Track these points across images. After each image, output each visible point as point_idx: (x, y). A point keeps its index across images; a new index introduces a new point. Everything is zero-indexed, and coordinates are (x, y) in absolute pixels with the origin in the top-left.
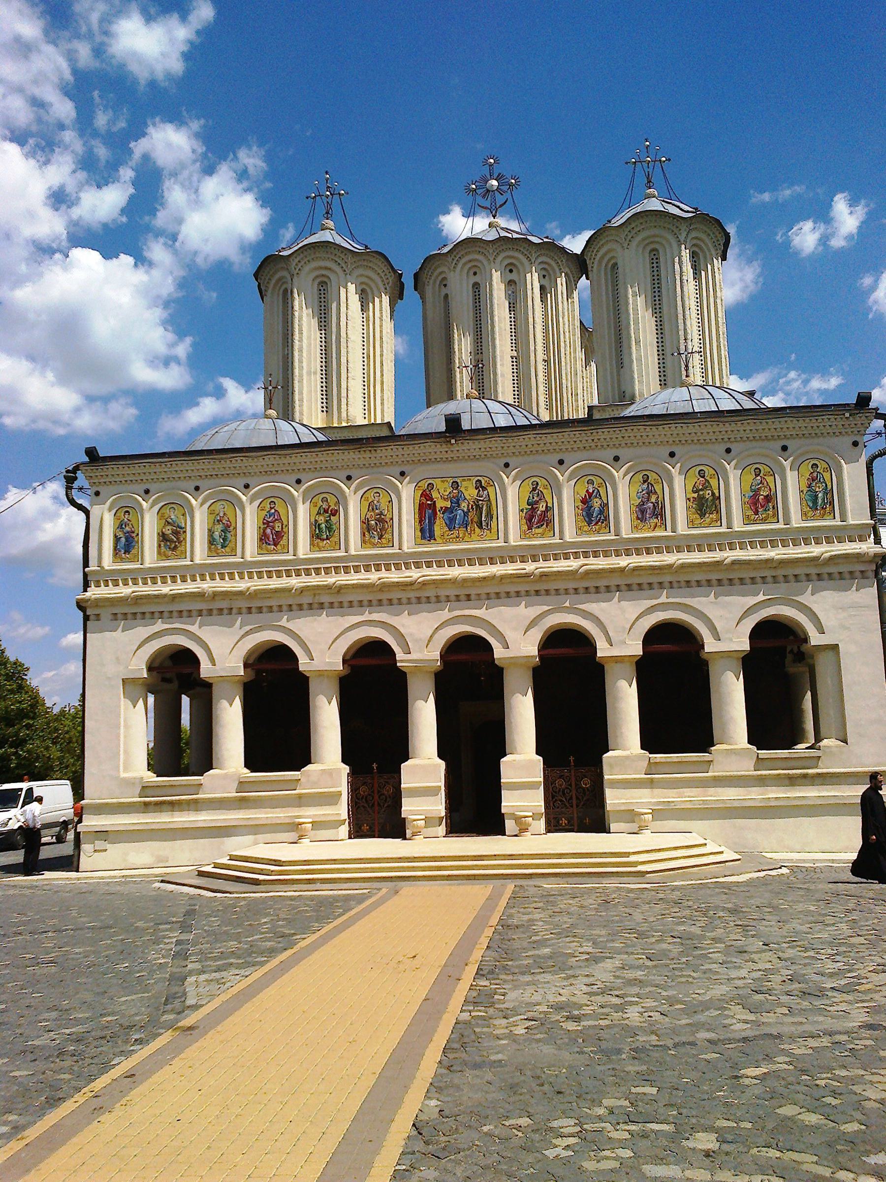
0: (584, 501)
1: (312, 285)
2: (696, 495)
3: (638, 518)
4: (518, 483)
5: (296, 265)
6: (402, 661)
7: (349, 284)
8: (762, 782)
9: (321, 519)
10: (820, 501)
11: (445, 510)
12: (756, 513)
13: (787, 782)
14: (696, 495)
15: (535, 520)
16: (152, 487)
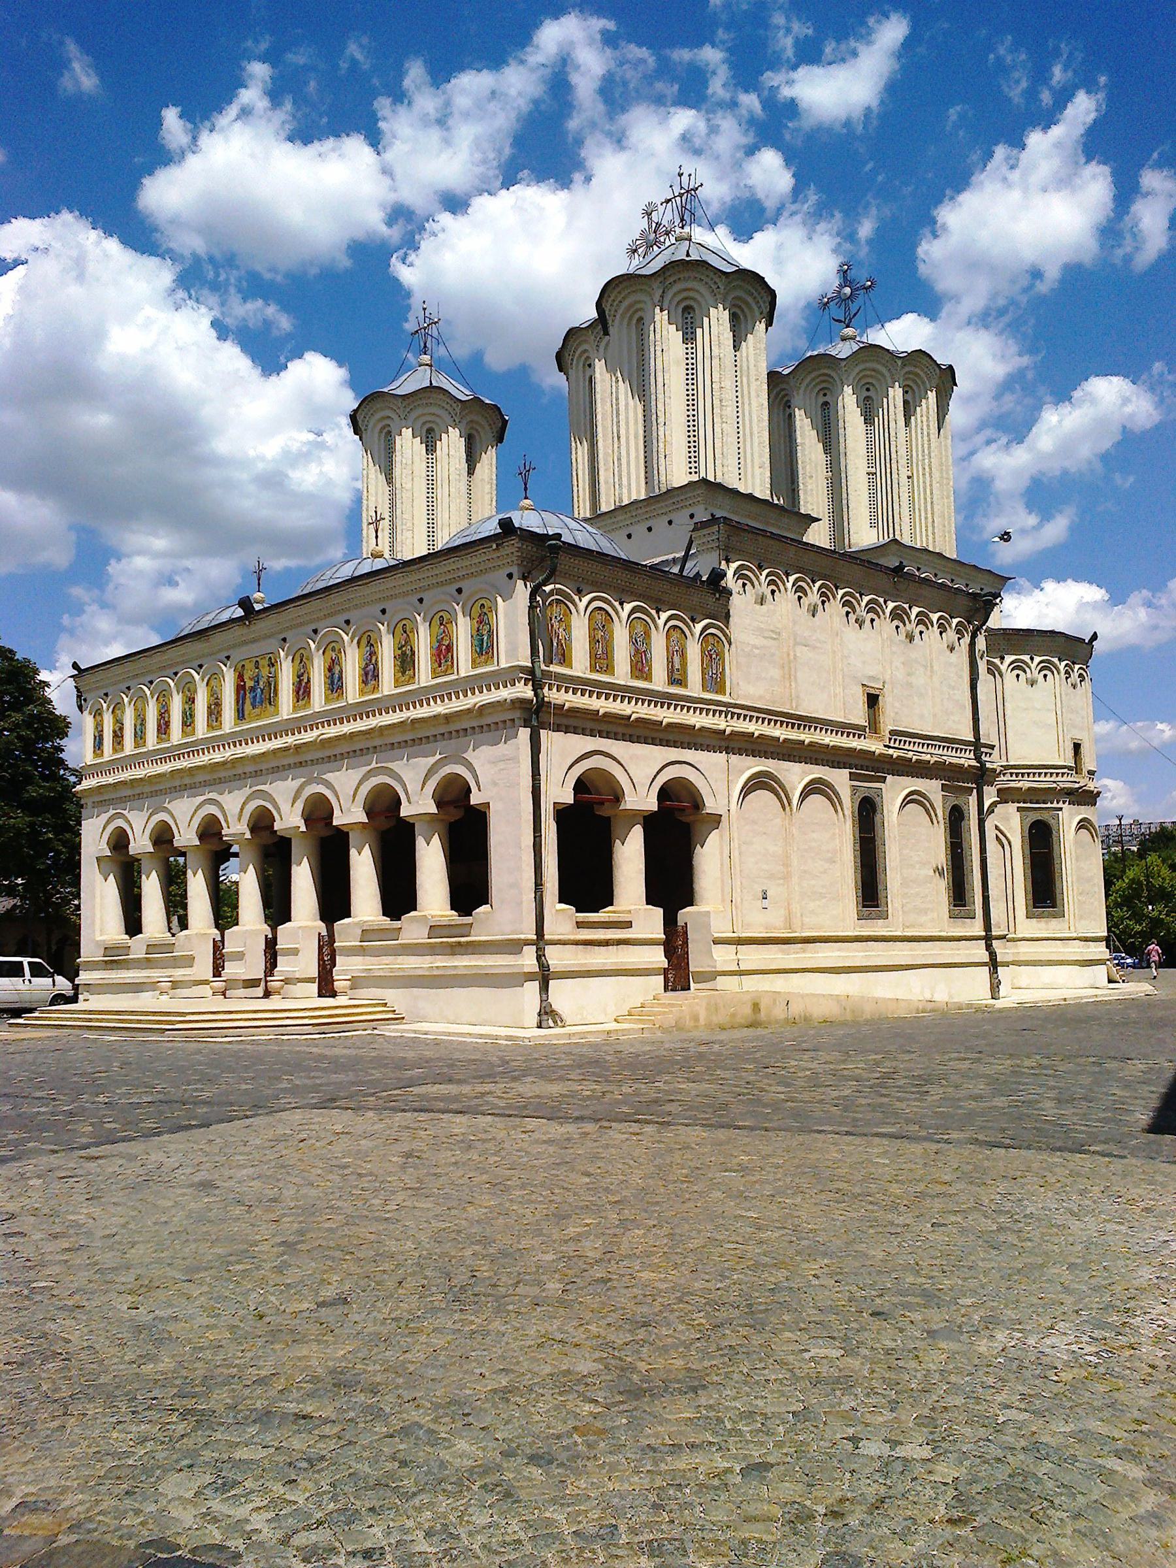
0: (330, 669)
1: (379, 440)
2: (400, 652)
3: (363, 682)
4: (290, 658)
5: (363, 421)
6: (226, 835)
7: (404, 430)
8: (432, 950)
9: (187, 707)
10: (485, 644)
11: (253, 689)
12: (440, 666)
13: (449, 950)
14: (400, 652)
15: (301, 693)
16: (109, 690)
